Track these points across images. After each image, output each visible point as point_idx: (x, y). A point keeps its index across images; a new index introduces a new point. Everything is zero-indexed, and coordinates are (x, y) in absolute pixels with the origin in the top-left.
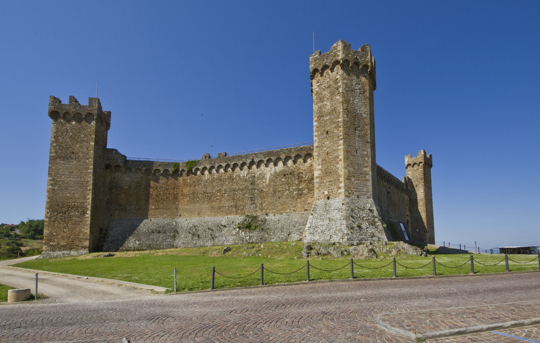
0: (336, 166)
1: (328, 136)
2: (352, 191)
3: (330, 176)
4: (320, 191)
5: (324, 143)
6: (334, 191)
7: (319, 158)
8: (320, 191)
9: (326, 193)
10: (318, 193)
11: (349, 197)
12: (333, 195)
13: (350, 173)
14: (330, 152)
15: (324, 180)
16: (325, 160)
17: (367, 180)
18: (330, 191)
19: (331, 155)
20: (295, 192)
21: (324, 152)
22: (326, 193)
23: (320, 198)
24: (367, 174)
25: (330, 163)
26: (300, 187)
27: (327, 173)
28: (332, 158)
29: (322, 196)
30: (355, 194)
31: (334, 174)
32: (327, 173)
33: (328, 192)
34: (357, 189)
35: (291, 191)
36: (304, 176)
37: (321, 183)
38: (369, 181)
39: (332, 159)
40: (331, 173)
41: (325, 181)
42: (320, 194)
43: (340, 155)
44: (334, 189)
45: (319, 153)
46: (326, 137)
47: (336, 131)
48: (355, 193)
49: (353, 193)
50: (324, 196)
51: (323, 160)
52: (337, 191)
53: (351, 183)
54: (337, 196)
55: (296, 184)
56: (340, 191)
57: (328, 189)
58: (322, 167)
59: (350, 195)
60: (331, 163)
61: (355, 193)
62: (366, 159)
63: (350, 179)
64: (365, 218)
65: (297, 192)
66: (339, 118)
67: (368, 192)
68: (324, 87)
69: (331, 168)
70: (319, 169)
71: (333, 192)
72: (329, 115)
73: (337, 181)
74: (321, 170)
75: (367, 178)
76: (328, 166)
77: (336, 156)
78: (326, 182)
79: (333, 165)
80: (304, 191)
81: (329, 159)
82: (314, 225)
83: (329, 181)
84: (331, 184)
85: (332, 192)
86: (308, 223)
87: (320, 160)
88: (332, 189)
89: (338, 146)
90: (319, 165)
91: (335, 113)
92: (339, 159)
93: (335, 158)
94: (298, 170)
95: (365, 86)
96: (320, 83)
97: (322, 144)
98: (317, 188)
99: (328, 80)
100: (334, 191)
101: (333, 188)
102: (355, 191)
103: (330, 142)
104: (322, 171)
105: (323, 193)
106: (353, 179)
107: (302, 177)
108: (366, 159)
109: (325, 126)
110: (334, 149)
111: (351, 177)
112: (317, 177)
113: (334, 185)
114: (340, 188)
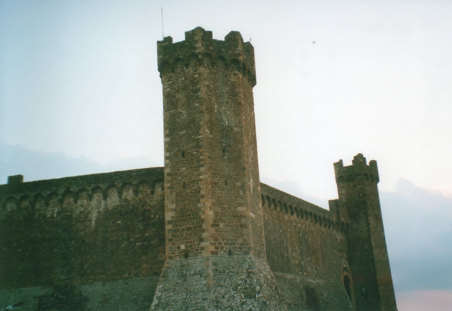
0: (196, 206)
1: (184, 159)
2: (220, 244)
3: (188, 220)
4: (174, 245)
5: (179, 170)
6: (195, 245)
7: (171, 192)
8: (174, 245)
9: (183, 247)
10: (171, 248)
11: (216, 253)
12: (192, 251)
13: (216, 216)
14: (187, 183)
15: (180, 226)
16: (181, 195)
18: (188, 245)
19: (189, 189)
20: (137, 244)
21: (179, 183)
22: (183, 247)
23: (173, 255)
25: (187, 201)
26: (147, 235)
27: (183, 216)
28: (190, 193)
29: (176, 252)
30: (224, 249)
31: (194, 218)
32: (183, 216)
33: (186, 246)
34: (228, 240)
35: (132, 242)
36: (152, 216)
37: (176, 231)
39: (190, 195)
40: (189, 215)
41: (181, 228)
42: (174, 249)
43: (202, 189)
44: (194, 242)
45: (172, 185)
46: (182, 161)
47: (196, 153)
49: (222, 248)
50: (180, 253)
51: (177, 195)
52: (199, 244)
54: (198, 252)
55: (139, 229)
56: (203, 244)
57: (185, 241)
58: (176, 206)
59: (218, 251)
60: (189, 200)
63: (218, 226)
64: (239, 287)
65: (140, 243)
66: (199, 135)
67: (244, 245)
68: (177, 88)
69: (189, 208)
70: (172, 210)
71: (193, 247)
72: (186, 128)
73: (198, 229)
74: (175, 210)
75: (242, 223)
76: (185, 205)
77: (196, 189)
78: (183, 230)
79: (192, 204)
80: (152, 242)
81: (187, 193)
82: (163, 301)
83: (188, 229)
84: (190, 234)
85: (191, 246)
86: (155, 298)
87: (174, 195)
88: (191, 242)
89: (199, 175)
90: (172, 202)
91: (193, 126)
92: (200, 195)
93: (194, 192)
94: (143, 206)
95: (235, 88)
96: (172, 82)
97: (176, 170)
98: (170, 240)
99: (183, 79)
100: (195, 245)
101: (192, 239)
102: (226, 244)
103: (188, 169)
104: (176, 212)
105: (179, 247)
106: (222, 225)
107: (150, 218)
109: (179, 143)
110: (193, 179)
111: (218, 221)
112: (170, 222)
113: (193, 234)
114: (202, 240)
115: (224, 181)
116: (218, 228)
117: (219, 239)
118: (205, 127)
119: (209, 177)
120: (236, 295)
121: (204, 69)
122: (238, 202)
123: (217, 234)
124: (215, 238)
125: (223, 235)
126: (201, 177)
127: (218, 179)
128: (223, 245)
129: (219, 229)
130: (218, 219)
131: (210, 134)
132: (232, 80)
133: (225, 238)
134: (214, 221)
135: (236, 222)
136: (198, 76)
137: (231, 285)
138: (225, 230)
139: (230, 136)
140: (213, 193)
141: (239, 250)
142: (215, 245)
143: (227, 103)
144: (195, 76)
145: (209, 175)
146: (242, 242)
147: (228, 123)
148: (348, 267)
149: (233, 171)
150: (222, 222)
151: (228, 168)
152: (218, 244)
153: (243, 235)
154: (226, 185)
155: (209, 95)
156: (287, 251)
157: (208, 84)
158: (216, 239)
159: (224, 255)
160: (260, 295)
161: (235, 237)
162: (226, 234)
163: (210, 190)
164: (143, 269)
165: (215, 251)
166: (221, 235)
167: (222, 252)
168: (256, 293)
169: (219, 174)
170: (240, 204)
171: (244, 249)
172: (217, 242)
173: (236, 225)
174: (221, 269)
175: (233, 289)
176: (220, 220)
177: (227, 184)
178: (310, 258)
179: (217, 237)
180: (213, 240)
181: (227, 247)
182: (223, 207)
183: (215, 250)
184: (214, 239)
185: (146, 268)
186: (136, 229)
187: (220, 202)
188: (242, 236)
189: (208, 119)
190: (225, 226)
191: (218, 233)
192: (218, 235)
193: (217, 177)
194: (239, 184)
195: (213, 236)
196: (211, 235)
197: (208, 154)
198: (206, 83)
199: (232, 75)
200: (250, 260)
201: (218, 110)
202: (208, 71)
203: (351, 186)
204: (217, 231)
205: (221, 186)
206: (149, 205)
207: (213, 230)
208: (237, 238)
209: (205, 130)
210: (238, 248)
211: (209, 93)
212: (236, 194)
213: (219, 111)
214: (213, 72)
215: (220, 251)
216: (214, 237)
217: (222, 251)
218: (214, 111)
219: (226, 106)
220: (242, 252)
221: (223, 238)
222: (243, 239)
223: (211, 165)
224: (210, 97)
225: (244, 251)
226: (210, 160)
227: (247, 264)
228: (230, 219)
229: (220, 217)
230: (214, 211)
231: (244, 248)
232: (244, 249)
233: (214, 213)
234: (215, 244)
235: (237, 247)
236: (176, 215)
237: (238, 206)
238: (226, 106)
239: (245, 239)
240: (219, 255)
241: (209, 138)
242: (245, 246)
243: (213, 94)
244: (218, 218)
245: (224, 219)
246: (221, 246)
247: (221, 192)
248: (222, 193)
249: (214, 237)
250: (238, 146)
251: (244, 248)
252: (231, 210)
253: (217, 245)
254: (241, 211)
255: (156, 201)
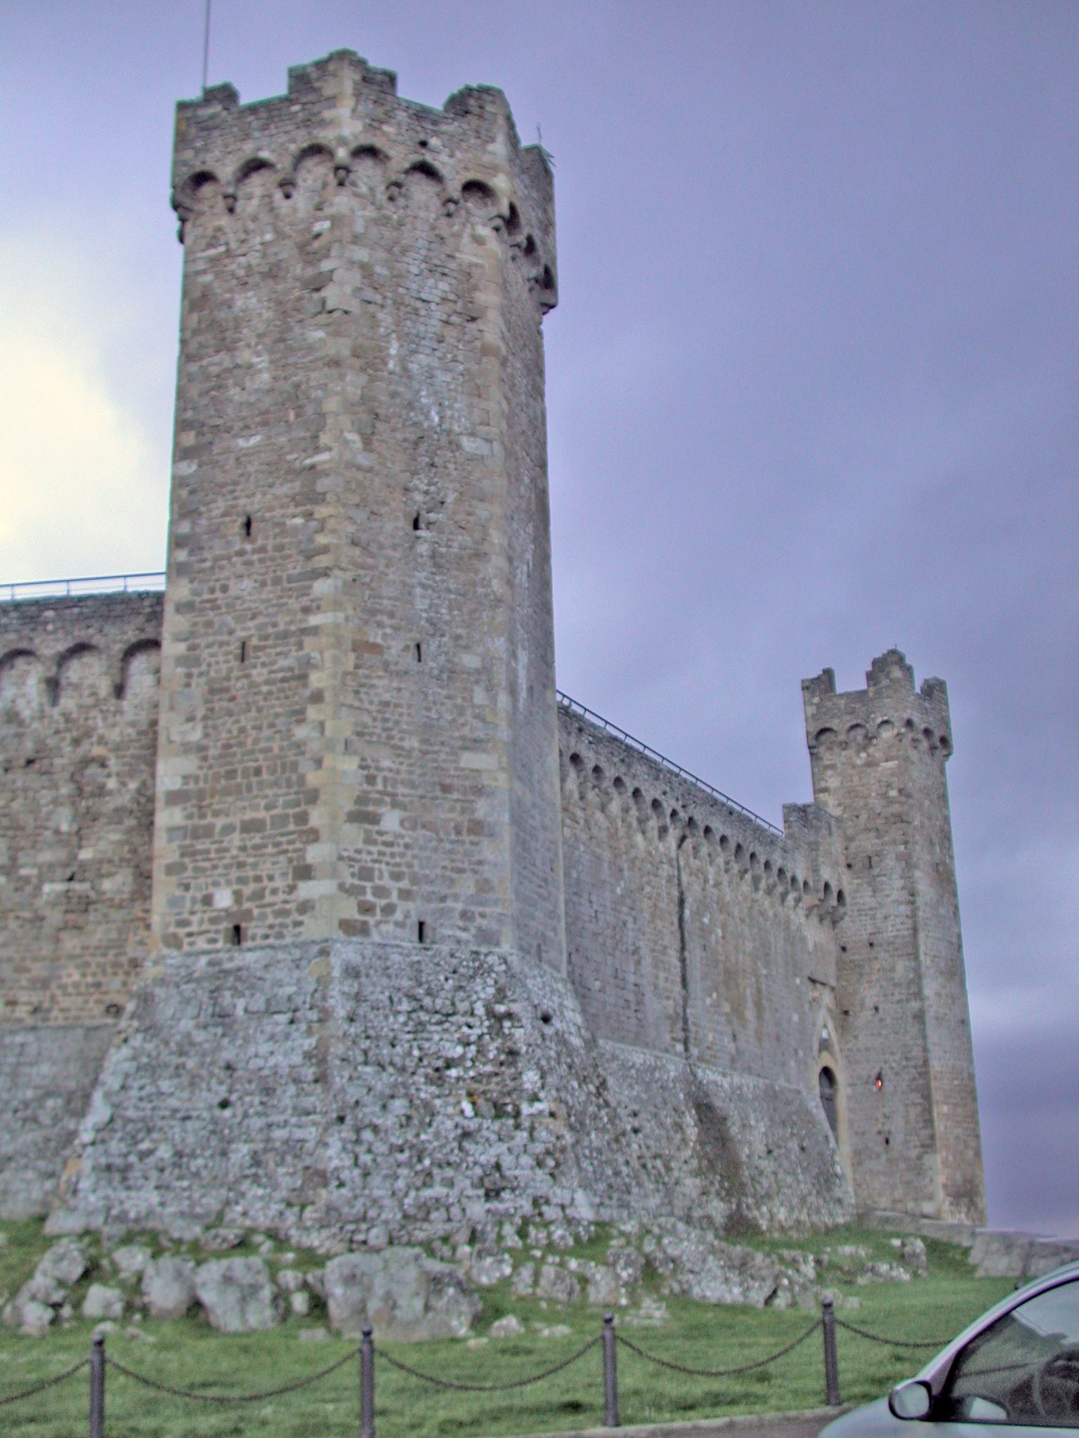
0: (288, 735)
1: (248, 547)
2: (380, 892)
3: (249, 789)
4: (187, 887)
5: (225, 589)
6: (274, 891)
7: (189, 676)
8: (187, 887)
9: (224, 899)
10: (174, 902)
11: (364, 930)
12: (263, 916)
13: (371, 780)
14: (255, 642)
15: (216, 814)
16: (227, 690)
17: (477, 827)
18: (248, 890)
19: (264, 665)
20: (47, 888)
21: (222, 644)
22: (224, 899)
23: (182, 931)
24: (479, 791)
25: (253, 713)
26: (85, 855)
27: (231, 774)
28: (267, 682)
29: (195, 919)
30: (398, 916)
31: (276, 784)
32: (231, 774)
33: (238, 896)
34: (415, 880)
35: (27, 880)
36: (112, 784)
37: (196, 834)
38: (492, 835)
39: (265, 689)
40: (258, 772)
41: (220, 822)
42: (188, 904)
43: (315, 667)
44: (271, 878)
45: (192, 648)
46: (241, 553)
47: (299, 521)
48: (402, 907)
49: (389, 910)
50: (213, 921)
51: (212, 691)
52: (292, 889)
53: (374, 842)
54: (288, 921)
55: (57, 832)
56: (306, 890)
57: (234, 874)
58: (206, 735)
59: (371, 920)
60: (259, 710)
61: (402, 907)
62: (480, 696)
63: (374, 819)
64: (453, 1072)
65: (60, 887)
66: (317, 450)
68: (241, 273)
69: (256, 741)
70: (187, 748)
71: (269, 899)
72: (265, 424)
73: (292, 827)
74: (200, 749)
75: (479, 815)
76: (242, 730)
77: (291, 669)
78: (228, 829)
79: (272, 725)
80: (107, 885)
81: (252, 685)
82: (131, 1113)
83: (250, 827)
84: (256, 847)
85: (258, 895)
86: (98, 1096)
87: (199, 687)
88: (258, 879)
89: (306, 610)
90: (191, 719)
91: (298, 416)
92: (307, 693)
93: (283, 680)
94: (76, 742)
95: (475, 288)
96: (222, 249)
97: (212, 591)
99: (269, 237)
100: (274, 891)
101: (266, 868)
102: (405, 895)
103: (263, 584)
104: (205, 759)
105: (208, 900)
106: (391, 821)
107: (101, 792)
108: (480, 696)
109: (236, 483)
110: (282, 627)
111: (379, 802)
112: (175, 798)
113: (270, 850)
114: (304, 872)
115: (412, 645)
116: (376, 828)
117: (377, 873)
118: (346, 421)
119: (347, 619)
120: (438, 1102)
121: (355, 202)
122: (466, 731)
123: (369, 853)
124: (362, 869)
125: (398, 860)
126: (314, 620)
127: (388, 631)
128: (394, 898)
129: (380, 833)
130: (379, 792)
131: (365, 449)
132: (464, 257)
133: (404, 869)
134: (362, 800)
135: (452, 810)
136: (326, 225)
137: (421, 1059)
138: (407, 840)
139: (445, 467)
140: (362, 685)
141: (461, 923)
142: (362, 898)
143: (440, 342)
144: (317, 228)
145: (350, 612)
146: (472, 891)
147: (442, 418)
148: (834, 1038)
149: (450, 609)
150: (395, 805)
151: (430, 592)
152: (374, 894)
153: (480, 863)
154: (419, 660)
155: (370, 303)
156: (638, 963)
157: (366, 260)
158: (366, 874)
159: (395, 938)
160: (538, 1106)
161: (444, 867)
162: (410, 853)
163: (350, 673)
164: (63, 987)
165: (356, 921)
166: (387, 859)
167: (389, 928)
168: (525, 1095)
169: (391, 615)
170: (475, 741)
171: (483, 923)
172: (368, 884)
173: (452, 824)
174: (381, 997)
175: (426, 1076)
176: (388, 799)
177: (423, 657)
178: (715, 995)
179: (370, 865)
180: (353, 875)
181: (411, 906)
182: (401, 748)
183: (358, 917)
184: (356, 870)
185: (76, 985)
186: (46, 828)
187: (390, 725)
188: (477, 867)
189: (359, 392)
190: (407, 825)
191: (374, 849)
192: (375, 857)
193: (380, 625)
194: (470, 661)
195: (351, 859)
196: (345, 854)
197: (351, 528)
198: (362, 254)
199: (466, 239)
200: (503, 967)
201: (403, 362)
202: (370, 212)
203: (859, 762)
204: (369, 841)
205: (397, 663)
206: (102, 741)
207: (353, 834)
208: (454, 875)
209: (342, 432)
210: (457, 915)
211: (369, 294)
212: (459, 701)
213: (405, 369)
214: (388, 218)
215: (378, 923)
216: (357, 866)
217: (386, 922)
218: (386, 364)
219: (434, 350)
220: (473, 931)
221: (396, 869)
222: (477, 881)
223: (361, 572)
224: (371, 308)
225: (480, 929)
226: (357, 552)
227: (490, 982)
228: (430, 795)
229: (385, 786)
230: (363, 759)
231: (483, 915)
232: (479, 921)
233: (362, 767)
234: (362, 890)
235: (451, 910)
236: (201, 768)
237: (465, 748)
238: (434, 350)
239: (487, 881)
240: (376, 937)
241: (359, 468)
242: (487, 910)
243: (385, 298)
244: (380, 787)
245: (403, 795)
246: (384, 902)
247: (395, 684)
248: (399, 689)
249: (357, 866)
250: (478, 512)
251: (483, 915)
252: (435, 760)
253: (369, 897)
254: (478, 771)
255: (132, 724)
